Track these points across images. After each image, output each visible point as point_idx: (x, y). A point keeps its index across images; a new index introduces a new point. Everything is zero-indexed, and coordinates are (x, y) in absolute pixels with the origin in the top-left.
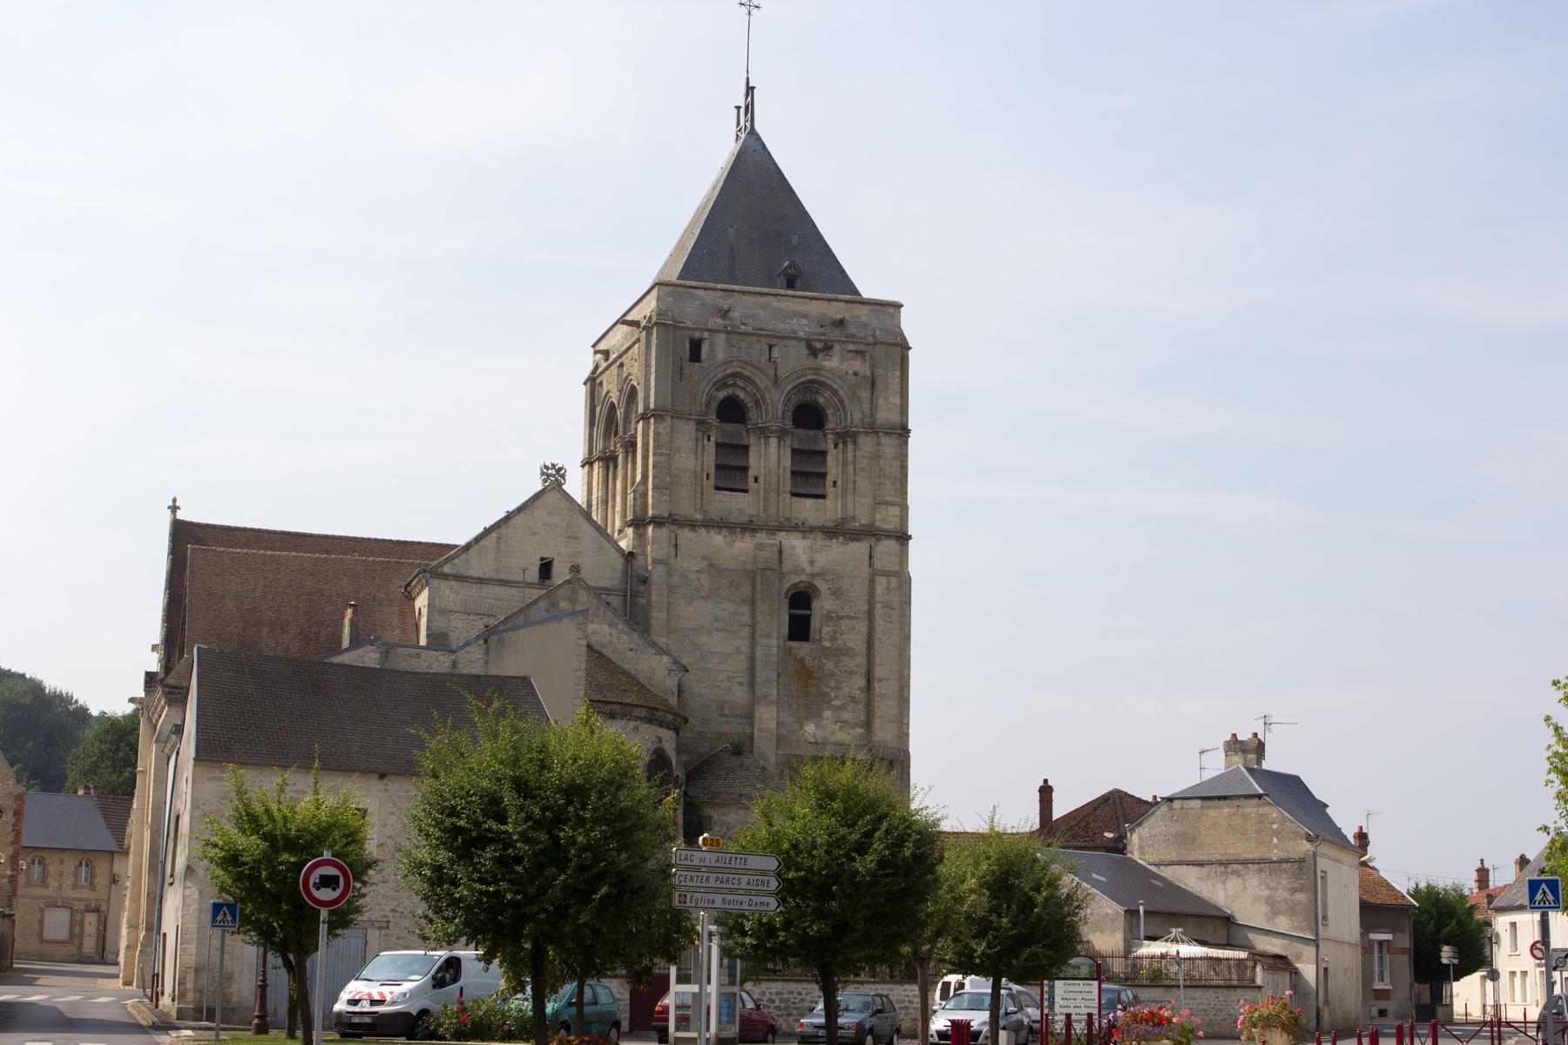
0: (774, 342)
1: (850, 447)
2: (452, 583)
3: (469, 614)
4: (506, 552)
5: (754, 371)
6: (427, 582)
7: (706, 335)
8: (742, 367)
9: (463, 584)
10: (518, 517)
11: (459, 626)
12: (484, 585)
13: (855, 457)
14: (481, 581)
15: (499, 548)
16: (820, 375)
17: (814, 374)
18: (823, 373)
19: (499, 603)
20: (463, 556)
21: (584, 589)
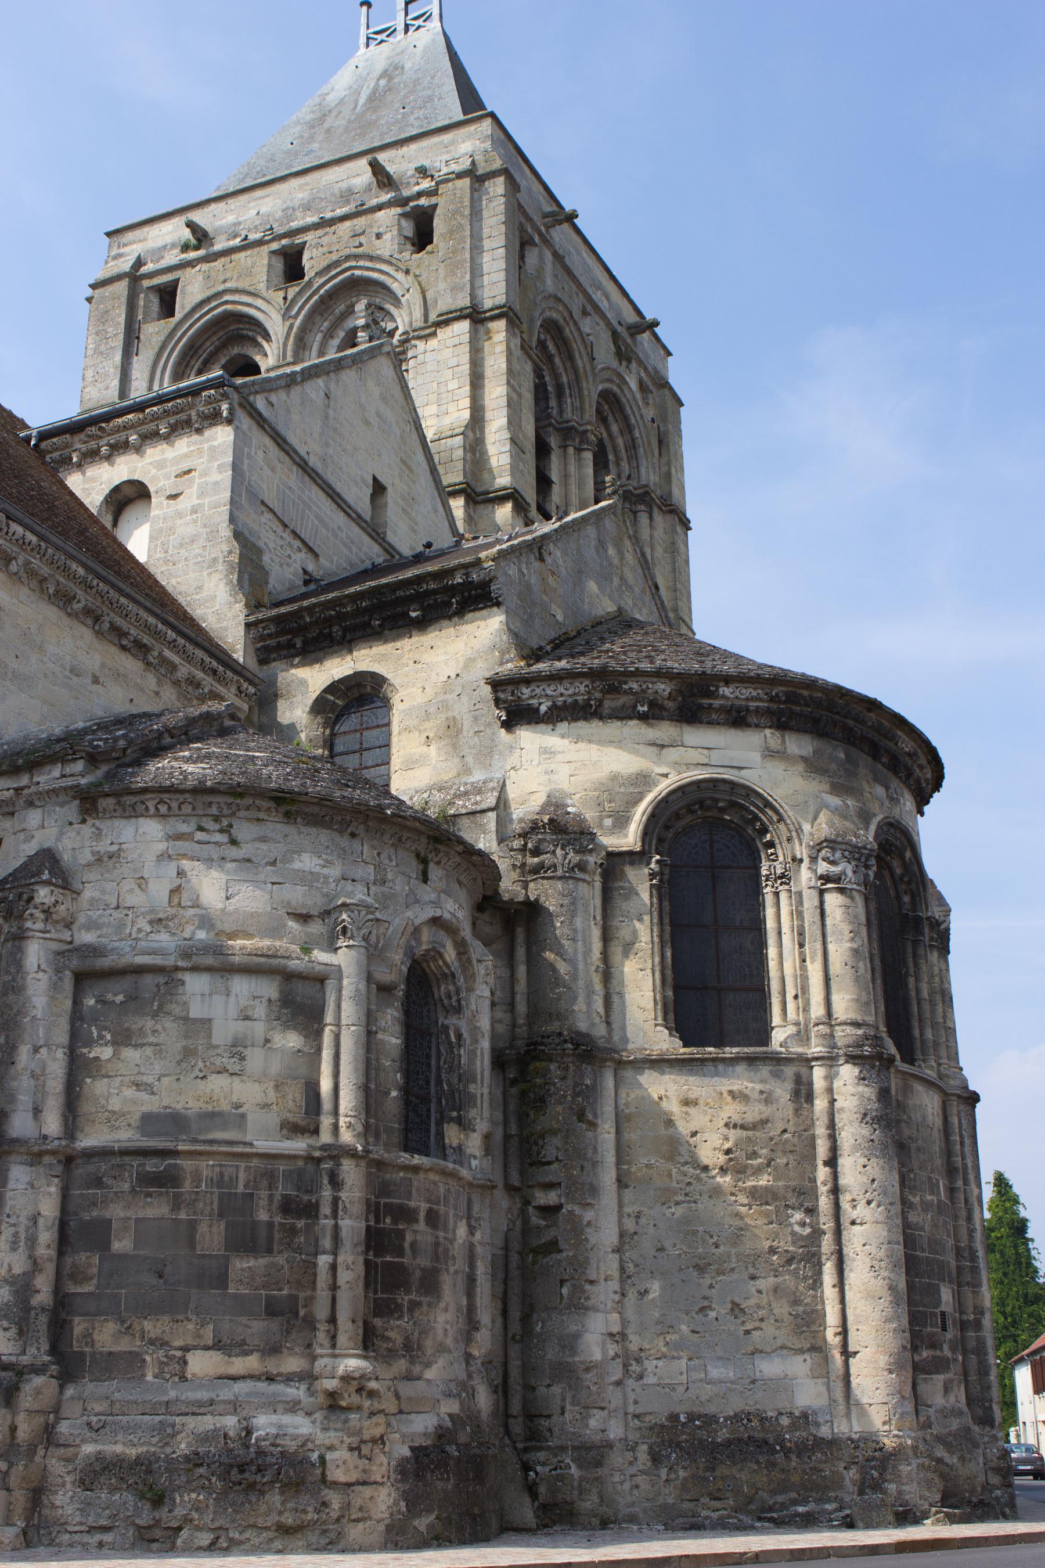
0: (589, 308)
1: (644, 519)
2: (267, 441)
3: (285, 526)
4: (335, 430)
5: (576, 335)
6: (231, 410)
7: (537, 239)
8: (565, 319)
9: (282, 454)
10: (348, 371)
11: (272, 545)
12: (307, 478)
13: (651, 537)
14: (303, 466)
15: (326, 417)
16: (622, 391)
17: (619, 386)
18: (626, 391)
19: (324, 531)
20: (282, 395)
21: (630, 537)
